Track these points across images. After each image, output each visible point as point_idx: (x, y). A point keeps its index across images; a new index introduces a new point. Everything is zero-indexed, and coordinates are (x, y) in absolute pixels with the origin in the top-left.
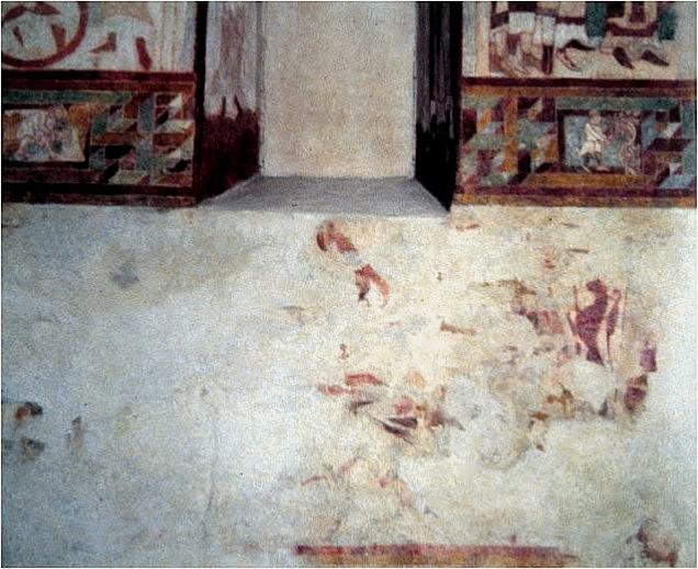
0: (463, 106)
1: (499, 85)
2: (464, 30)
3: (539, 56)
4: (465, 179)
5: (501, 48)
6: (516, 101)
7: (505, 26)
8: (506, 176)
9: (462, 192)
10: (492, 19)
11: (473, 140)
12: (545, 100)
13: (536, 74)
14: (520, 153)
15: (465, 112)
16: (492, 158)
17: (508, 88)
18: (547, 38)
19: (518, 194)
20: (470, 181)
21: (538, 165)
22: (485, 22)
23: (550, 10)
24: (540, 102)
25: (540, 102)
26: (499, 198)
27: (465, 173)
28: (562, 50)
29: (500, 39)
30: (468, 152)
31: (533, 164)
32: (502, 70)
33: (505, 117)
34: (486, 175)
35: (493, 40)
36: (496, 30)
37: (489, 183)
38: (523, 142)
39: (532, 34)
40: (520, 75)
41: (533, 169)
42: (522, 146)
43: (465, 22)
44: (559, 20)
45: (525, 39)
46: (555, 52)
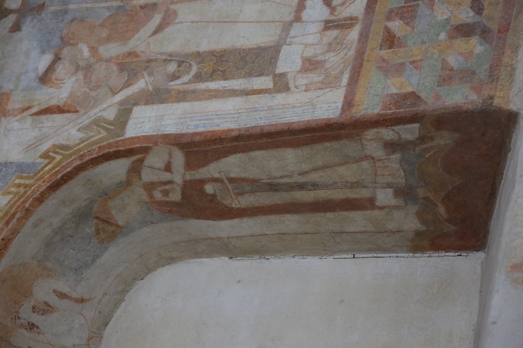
0: (377, 111)
1: (359, 72)
2: (284, 121)
3: (335, 33)
4: (474, 97)
5: (315, 77)
6: (383, 53)
7: (289, 76)
8: (479, 49)
9: (492, 98)
10: (279, 91)
11: (423, 95)
12: (389, 17)
13: (354, 34)
14: (451, 37)
15: (385, 108)
16: (452, 70)
17: (365, 64)
18: (315, 28)
19: (507, 31)
20: (477, 90)
21: (472, 14)
22: (280, 98)
23: (283, 31)
24: (390, 25)
25: (390, 25)
26: (508, 52)
27: (467, 97)
28: (333, 9)
29: (303, 81)
30: (438, 97)
31: (469, 21)
32: (338, 77)
33: (400, 61)
34: (474, 73)
35: (303, 88)
36: (291, 86)
37: (486, 67)
38: (438, 35)
39: (306, 45)
40: (352, 52)
41: (477, 18)
42: (443, 36)
43: (274, 121)
44: (298, 19)
45: (309, 52)
46: (333, 18)
